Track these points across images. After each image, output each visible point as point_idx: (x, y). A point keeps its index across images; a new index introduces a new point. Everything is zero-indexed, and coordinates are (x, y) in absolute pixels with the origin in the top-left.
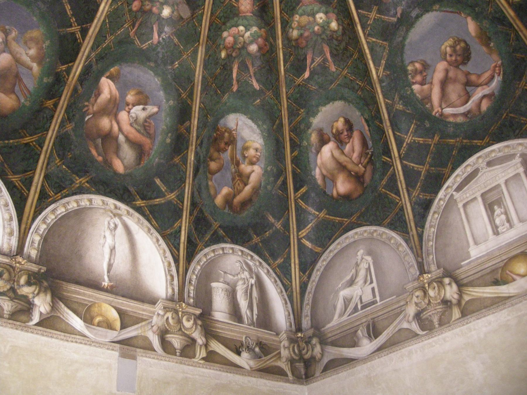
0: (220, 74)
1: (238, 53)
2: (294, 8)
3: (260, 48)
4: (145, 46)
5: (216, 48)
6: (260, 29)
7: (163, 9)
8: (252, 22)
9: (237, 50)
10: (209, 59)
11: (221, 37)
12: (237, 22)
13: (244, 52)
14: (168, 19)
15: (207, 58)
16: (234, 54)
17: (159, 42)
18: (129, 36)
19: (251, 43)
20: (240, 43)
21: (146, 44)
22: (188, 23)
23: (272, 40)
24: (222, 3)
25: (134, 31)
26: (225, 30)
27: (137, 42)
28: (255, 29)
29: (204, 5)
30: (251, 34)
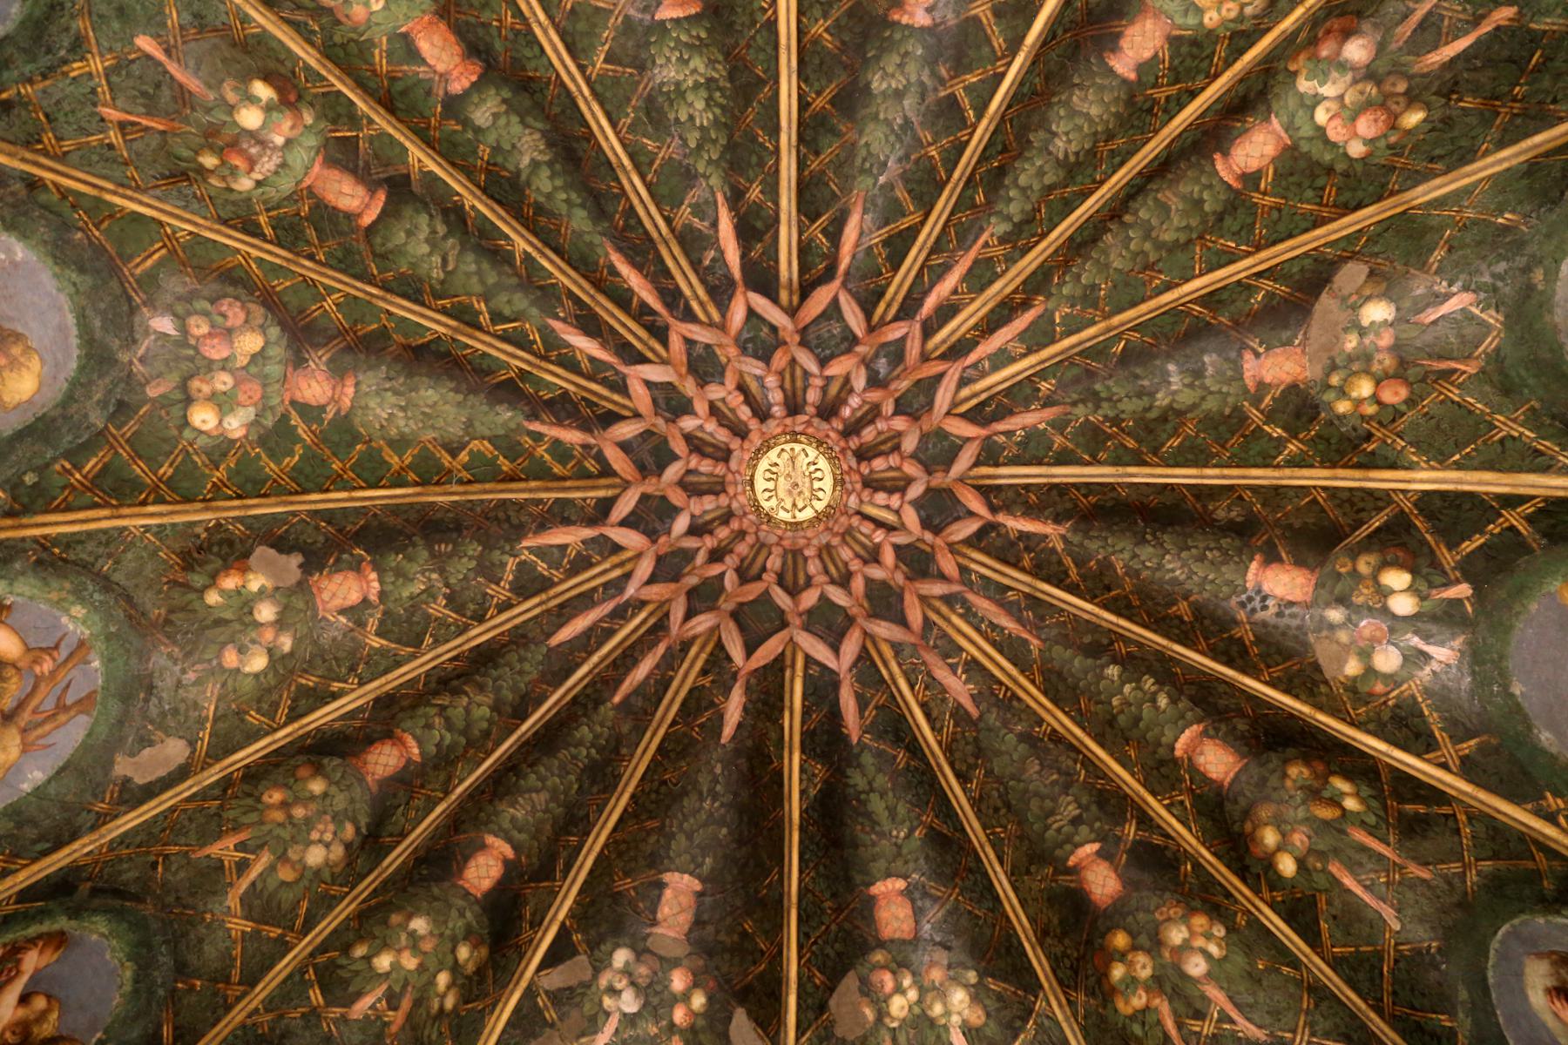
0: (1475, 92)
1: (1392, 79)
2: (1194, 42)
3: (1347, 34)
4: (1492, 318)
5: (1401, 155)
6: (1295, 74)
7: (1373, 323)
8: (1292, 102)
9: (1387, 87)
10: (1441, 157)
11: (1369, 155)
12: (1310, 139)
13: (1382, 67)
14: (1391, 300)
15: (1439, 166)
16: (1401, 87)
17: (1466, 289)
18: (1483, 371)
19: (1343, 66)
20: (1362, 93)
21: (1483, 316)
22: (1376, 255)
23: (1303, 35)
24: (1279, 210)
25: (1462, 367)
26: (1346, 155)
27: (1489, 343)
28: (1304, 85)
29: (1306, 254)
30: (1322, 84)
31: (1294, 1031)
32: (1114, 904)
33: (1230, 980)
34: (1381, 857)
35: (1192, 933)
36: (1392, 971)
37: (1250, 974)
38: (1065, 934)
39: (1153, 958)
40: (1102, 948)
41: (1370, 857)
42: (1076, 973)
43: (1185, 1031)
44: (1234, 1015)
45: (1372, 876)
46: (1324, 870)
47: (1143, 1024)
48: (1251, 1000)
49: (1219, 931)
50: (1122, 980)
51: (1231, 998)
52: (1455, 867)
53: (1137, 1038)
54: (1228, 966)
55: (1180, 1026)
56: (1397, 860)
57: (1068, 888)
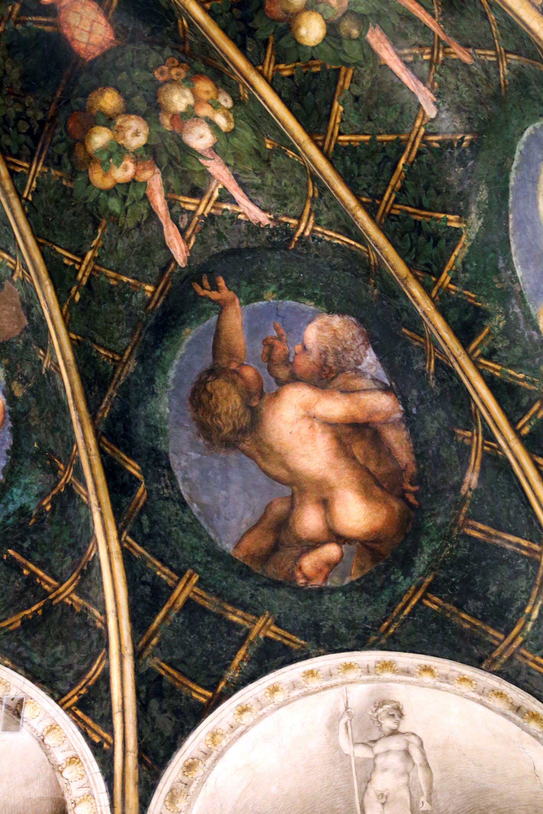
31: (299, 218)
32: (104, 55)
33: (237, 156)
34: (426, 30)
35: (197, 100)
36: (409, 166)
37: (258, 153)
38: (26, 91)
39: (149, 125)
40: (83, 109)
41: (416, 28)
42: (36, 139)
43: (176, 209)
44: (238, 194)
45: (416, 51)
46: (361, 40)
47: (125, 199)
48: (257, 180)
49: (226, 101)
50: (103, 149)
51: (236, 177)
52: (489, 55)
53: (112, 214)
54: (235, 141)
55: (171, 204)
56: (443, 37)
57: (39, 33)
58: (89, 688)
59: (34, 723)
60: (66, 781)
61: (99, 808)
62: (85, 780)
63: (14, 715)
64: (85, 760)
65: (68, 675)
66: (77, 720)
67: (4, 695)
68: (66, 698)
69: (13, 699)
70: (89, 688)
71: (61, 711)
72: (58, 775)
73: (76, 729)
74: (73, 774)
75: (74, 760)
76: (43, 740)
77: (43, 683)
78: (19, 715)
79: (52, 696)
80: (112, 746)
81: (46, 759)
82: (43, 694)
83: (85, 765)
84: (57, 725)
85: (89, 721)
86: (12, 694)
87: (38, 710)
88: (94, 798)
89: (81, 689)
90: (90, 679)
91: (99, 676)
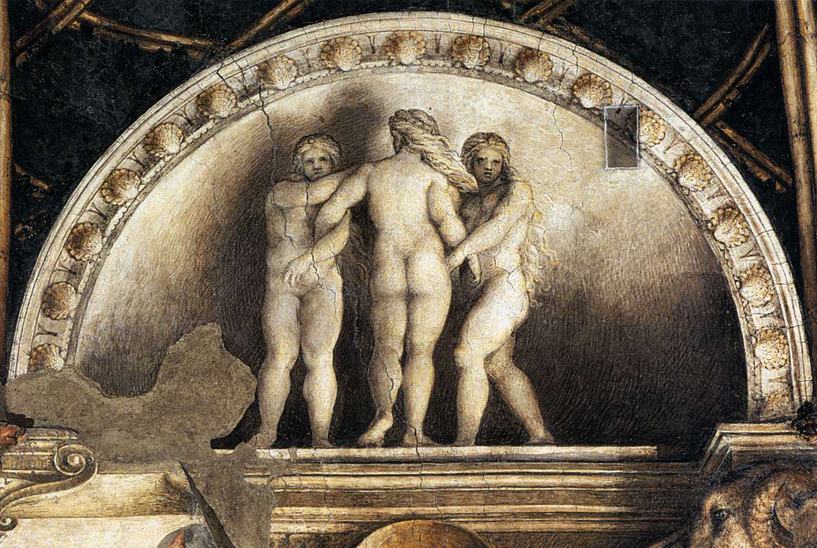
58: (742, 90)
59: (658, 150)
60: (722, 247)
61: (777, 287)
62: (750, 245)
63: (626, 138)
64: (747, 210)
65: (704, 67)
66: (726, 145)
67: (603, 105)
68: (704, 108)
69: (618, 111)
70: (742, 90)
71: (698, 129)
72: (708, 236)
73: (726, 160)
74: (732, 234)
75: (730, 211)
76: (677, 179)
77: (664, 81)
78: (632, 139)
79: (682, 105)
80: (793, 191)
81: (686, 211)
82: (666, 100)
83: (748, 219)
84: (696, 154)
85: (748, 147)
86: (617, 101)
87: (662, 129)
88: (769, 273)
89: (729, 91)
90: (743, 74)
91: (759, 69)
